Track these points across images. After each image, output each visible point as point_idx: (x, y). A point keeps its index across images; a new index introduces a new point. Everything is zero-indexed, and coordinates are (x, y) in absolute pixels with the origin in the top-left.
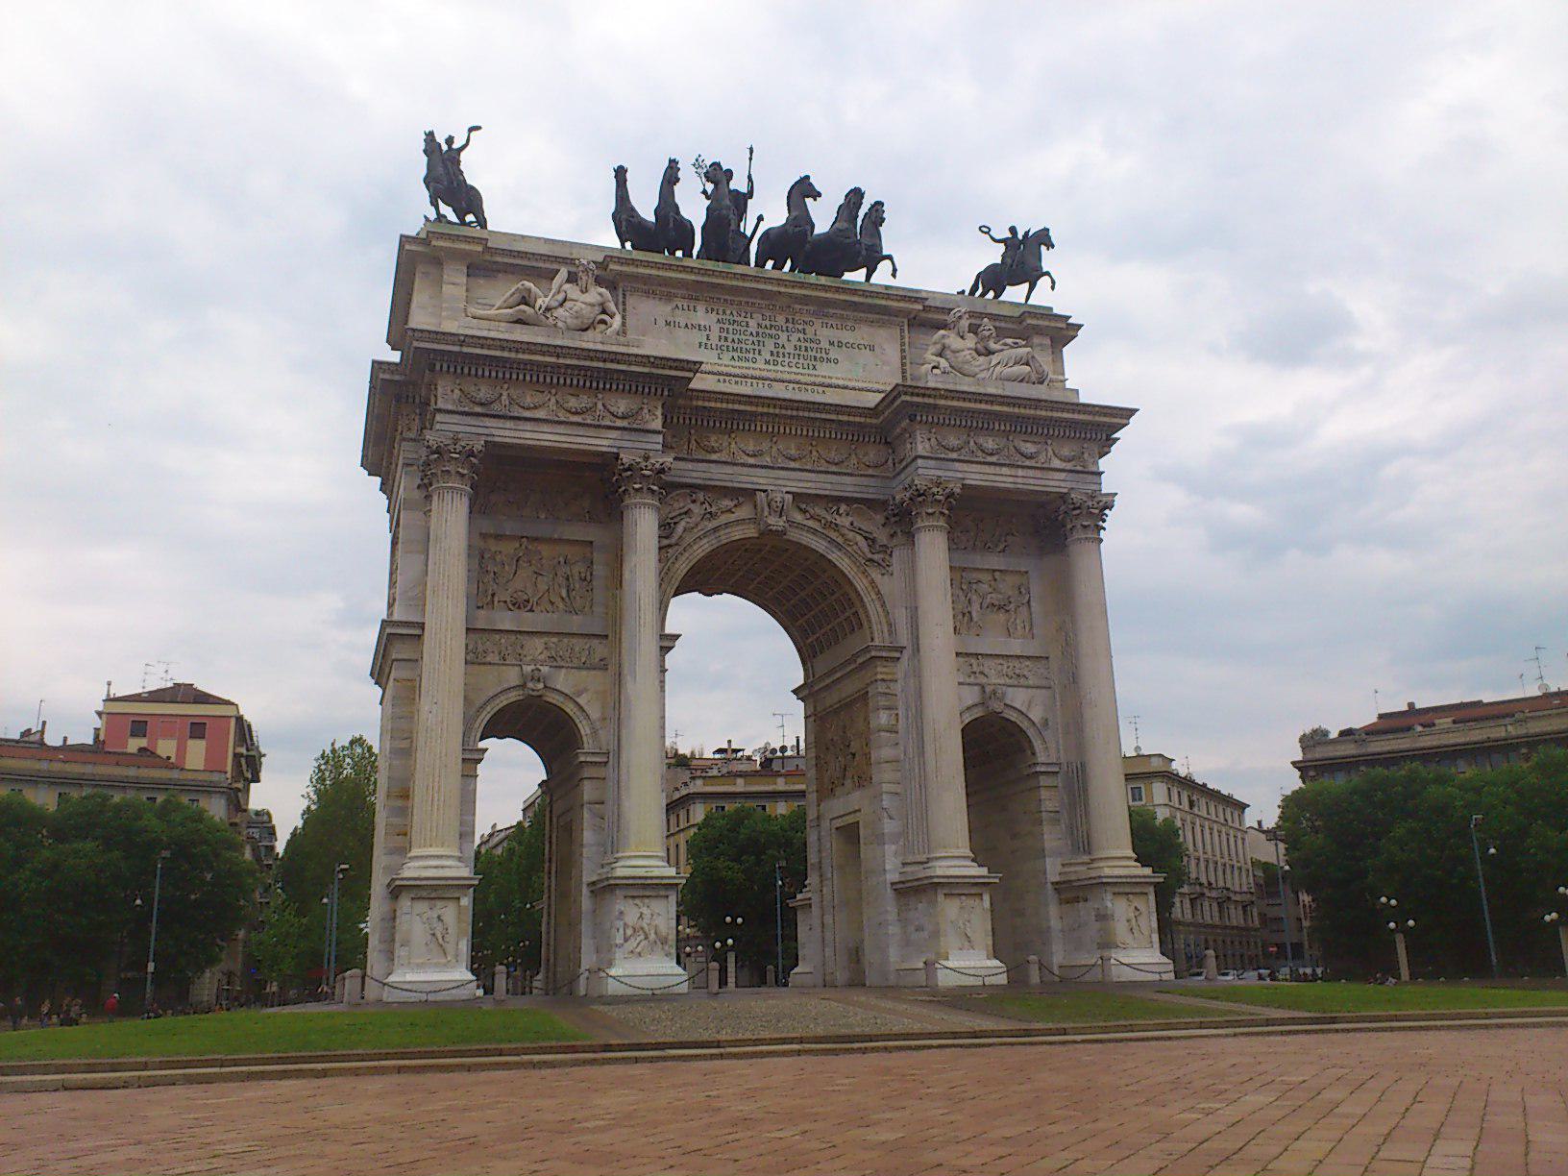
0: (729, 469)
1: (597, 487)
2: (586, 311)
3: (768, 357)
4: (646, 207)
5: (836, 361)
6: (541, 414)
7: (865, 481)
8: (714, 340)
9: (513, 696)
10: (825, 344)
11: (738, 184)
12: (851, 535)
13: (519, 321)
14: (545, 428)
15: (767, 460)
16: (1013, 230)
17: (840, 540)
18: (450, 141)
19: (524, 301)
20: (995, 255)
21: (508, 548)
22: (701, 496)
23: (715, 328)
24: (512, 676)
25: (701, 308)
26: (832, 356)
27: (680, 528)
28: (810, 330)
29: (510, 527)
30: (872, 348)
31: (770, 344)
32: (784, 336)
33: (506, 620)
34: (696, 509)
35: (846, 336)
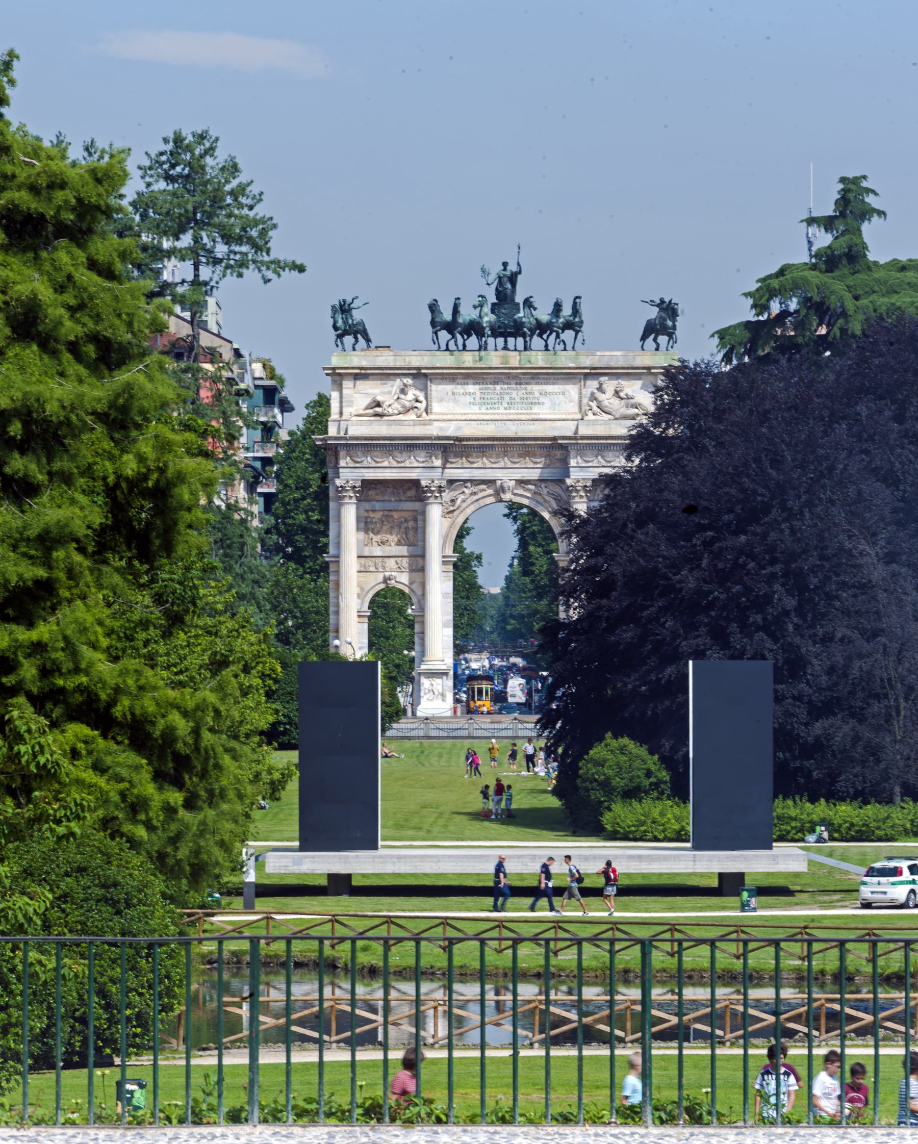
0: (483, 471)
1: (414, 491)
2: (408, 404)
3: (506, 405)
4: (448, 316)
5: (543, 404)
6: (386, 464)
7: (554, 470)
8: (478, 400)
9: (383, 586)
10: (537, 394)
11: (512, 267)
12: (547, 498)
13: (377, 415)
14: (387, 470)
15: (502, 464)
16: (662, 301)
17: (541, 501)
18: (344, 301)
19: (378, 405)
20: (653, 313)
21: (378, 515)
22: (469, 484)
23: (478, 395)
24: (380, 577)
25: (471, 381)
26: (542, 399)
27: (458, 502)
28: (529, 387)
29: (378, 506)
30: (564, 394)
31: (507, 398)
32: (514, 393)
33: (378, 551)
34: (466, 491)
35: (550, 388)
